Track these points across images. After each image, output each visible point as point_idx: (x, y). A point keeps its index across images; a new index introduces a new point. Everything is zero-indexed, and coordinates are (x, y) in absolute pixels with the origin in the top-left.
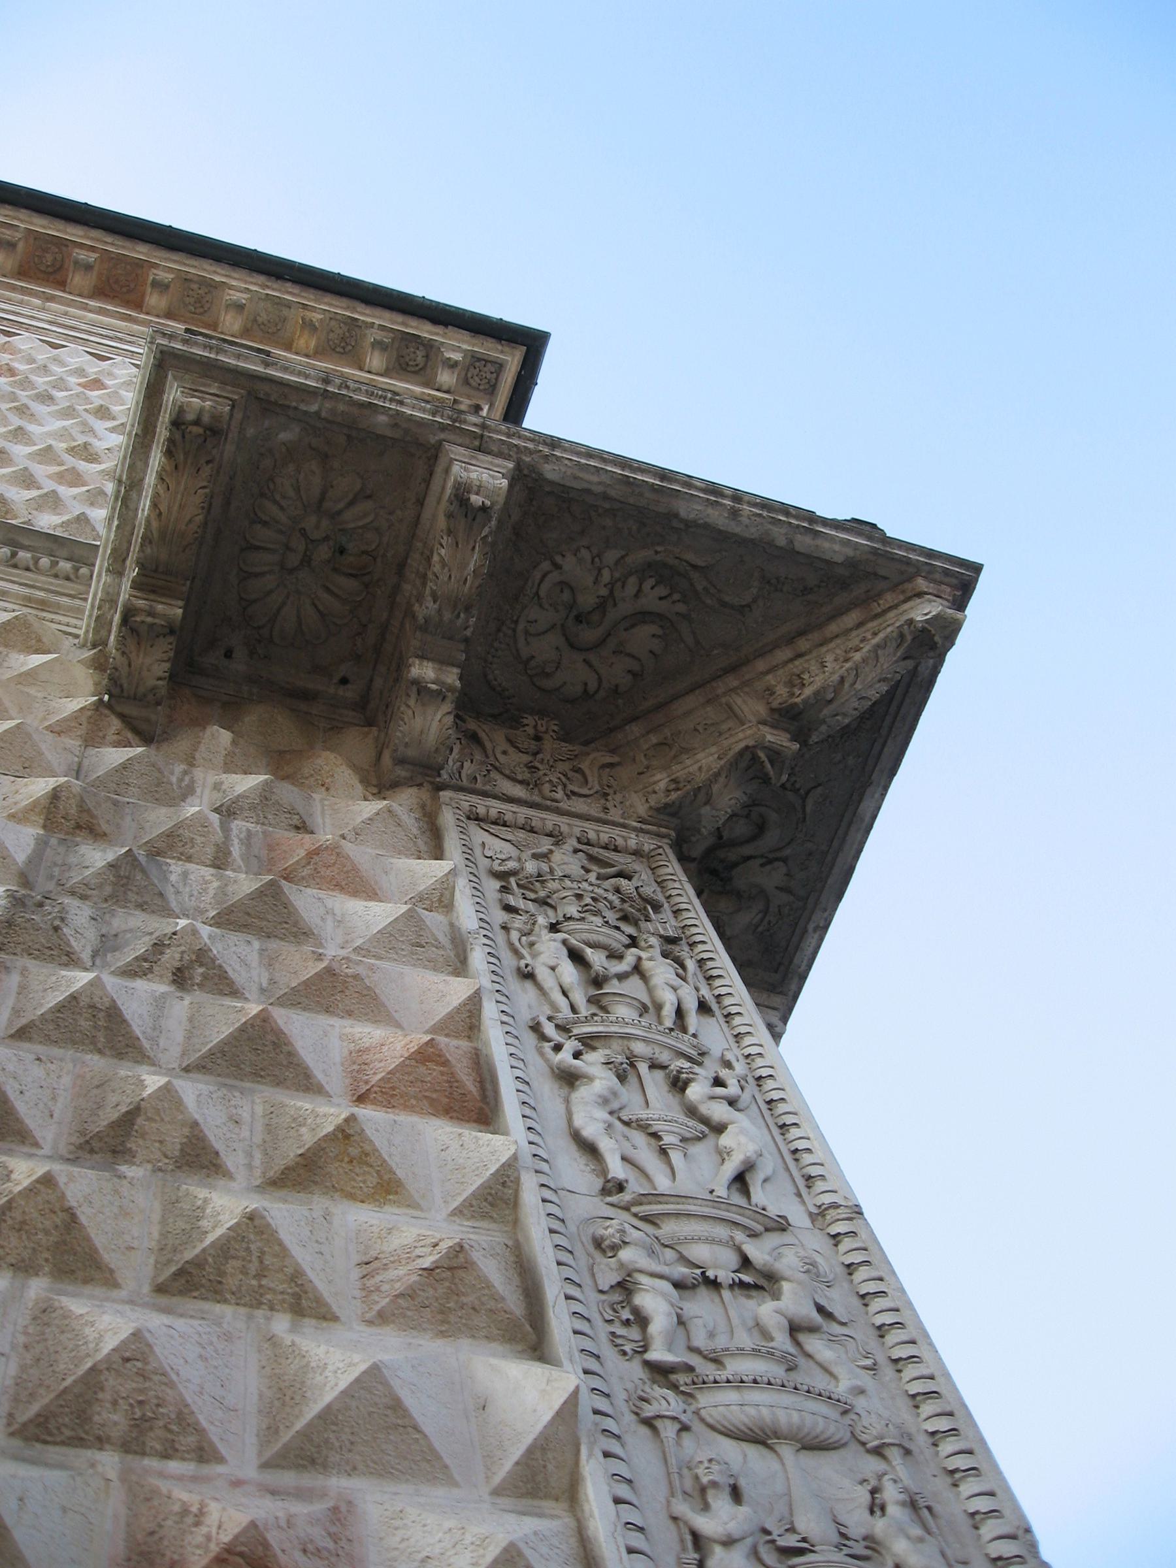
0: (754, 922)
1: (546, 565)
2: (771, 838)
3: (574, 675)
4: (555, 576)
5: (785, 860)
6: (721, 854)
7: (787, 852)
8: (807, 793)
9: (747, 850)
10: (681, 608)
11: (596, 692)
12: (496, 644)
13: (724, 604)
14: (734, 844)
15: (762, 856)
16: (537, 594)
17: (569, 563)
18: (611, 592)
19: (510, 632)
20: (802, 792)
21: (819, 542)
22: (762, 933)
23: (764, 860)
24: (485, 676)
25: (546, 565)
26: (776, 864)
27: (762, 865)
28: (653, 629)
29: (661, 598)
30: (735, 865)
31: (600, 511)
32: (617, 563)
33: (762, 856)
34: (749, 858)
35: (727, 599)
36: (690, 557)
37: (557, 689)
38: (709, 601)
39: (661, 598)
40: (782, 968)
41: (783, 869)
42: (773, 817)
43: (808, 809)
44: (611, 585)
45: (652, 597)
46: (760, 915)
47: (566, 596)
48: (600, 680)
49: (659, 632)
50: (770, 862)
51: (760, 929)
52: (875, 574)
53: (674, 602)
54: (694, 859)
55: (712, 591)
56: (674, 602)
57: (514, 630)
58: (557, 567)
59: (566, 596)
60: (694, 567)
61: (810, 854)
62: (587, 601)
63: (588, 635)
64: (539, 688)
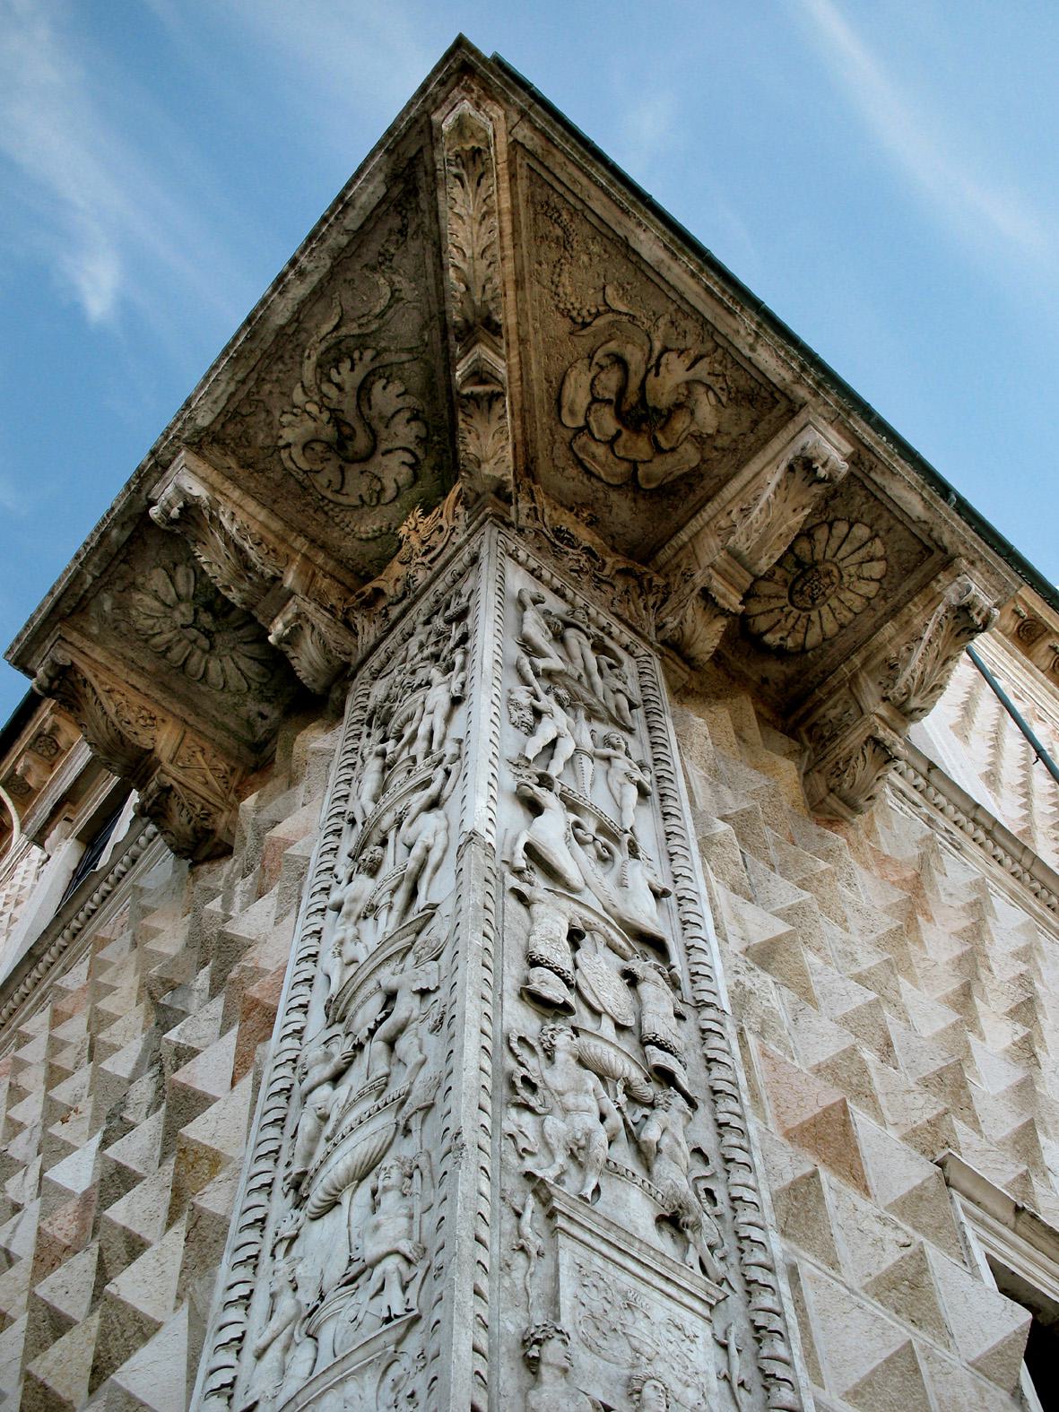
0: (713, 401)
1: (284, 454)
2: (635, 356)
4: (296, 452)
5: (665, 350)
6: (626, 407)
7: (658, 346)
8: (606, 304)
9: (634, 383)
10: (369, 354)
12: (337, 520)
13: (382, 315)
14: (622, 391)
15: (648, 371)
16: (305, 472)
17: (288, 435)
18: (328, 409)
19: (331, 506)
20: (601, 309)
21: (358, 204)
22: (729, 399)
23: (653, 371)
24: (361, 539)
25: (284, 454)
26: (663, 361)
29: (352, 369)
30: (642, 399)
31: (254, 390)
32: (305, 393)
33: (648, 371)
35: (377, 310)
36: (327, 328)
37: (398, 488)
38: (374, 327)
39: (352, 369)
40: (777, 395)
41: (671, 357)
42: (612, 346)
43: (623, 309)
44: (321, 407)
45: (348, 376)
46: (711, 394)
48: (405, 449)
49: (383, 382)
50: (658, 365)
51: (724, 399)
52: (411, 159)
53: (361, 359)
54: (619, 433)
55: (364, 320)
56: (361, 359)
57: (330, 501)
58: (288, 446)
59: (318, 447)
60: (337, 328)
61: (672, 323)
62: (329, 432)
63: (361, 442)
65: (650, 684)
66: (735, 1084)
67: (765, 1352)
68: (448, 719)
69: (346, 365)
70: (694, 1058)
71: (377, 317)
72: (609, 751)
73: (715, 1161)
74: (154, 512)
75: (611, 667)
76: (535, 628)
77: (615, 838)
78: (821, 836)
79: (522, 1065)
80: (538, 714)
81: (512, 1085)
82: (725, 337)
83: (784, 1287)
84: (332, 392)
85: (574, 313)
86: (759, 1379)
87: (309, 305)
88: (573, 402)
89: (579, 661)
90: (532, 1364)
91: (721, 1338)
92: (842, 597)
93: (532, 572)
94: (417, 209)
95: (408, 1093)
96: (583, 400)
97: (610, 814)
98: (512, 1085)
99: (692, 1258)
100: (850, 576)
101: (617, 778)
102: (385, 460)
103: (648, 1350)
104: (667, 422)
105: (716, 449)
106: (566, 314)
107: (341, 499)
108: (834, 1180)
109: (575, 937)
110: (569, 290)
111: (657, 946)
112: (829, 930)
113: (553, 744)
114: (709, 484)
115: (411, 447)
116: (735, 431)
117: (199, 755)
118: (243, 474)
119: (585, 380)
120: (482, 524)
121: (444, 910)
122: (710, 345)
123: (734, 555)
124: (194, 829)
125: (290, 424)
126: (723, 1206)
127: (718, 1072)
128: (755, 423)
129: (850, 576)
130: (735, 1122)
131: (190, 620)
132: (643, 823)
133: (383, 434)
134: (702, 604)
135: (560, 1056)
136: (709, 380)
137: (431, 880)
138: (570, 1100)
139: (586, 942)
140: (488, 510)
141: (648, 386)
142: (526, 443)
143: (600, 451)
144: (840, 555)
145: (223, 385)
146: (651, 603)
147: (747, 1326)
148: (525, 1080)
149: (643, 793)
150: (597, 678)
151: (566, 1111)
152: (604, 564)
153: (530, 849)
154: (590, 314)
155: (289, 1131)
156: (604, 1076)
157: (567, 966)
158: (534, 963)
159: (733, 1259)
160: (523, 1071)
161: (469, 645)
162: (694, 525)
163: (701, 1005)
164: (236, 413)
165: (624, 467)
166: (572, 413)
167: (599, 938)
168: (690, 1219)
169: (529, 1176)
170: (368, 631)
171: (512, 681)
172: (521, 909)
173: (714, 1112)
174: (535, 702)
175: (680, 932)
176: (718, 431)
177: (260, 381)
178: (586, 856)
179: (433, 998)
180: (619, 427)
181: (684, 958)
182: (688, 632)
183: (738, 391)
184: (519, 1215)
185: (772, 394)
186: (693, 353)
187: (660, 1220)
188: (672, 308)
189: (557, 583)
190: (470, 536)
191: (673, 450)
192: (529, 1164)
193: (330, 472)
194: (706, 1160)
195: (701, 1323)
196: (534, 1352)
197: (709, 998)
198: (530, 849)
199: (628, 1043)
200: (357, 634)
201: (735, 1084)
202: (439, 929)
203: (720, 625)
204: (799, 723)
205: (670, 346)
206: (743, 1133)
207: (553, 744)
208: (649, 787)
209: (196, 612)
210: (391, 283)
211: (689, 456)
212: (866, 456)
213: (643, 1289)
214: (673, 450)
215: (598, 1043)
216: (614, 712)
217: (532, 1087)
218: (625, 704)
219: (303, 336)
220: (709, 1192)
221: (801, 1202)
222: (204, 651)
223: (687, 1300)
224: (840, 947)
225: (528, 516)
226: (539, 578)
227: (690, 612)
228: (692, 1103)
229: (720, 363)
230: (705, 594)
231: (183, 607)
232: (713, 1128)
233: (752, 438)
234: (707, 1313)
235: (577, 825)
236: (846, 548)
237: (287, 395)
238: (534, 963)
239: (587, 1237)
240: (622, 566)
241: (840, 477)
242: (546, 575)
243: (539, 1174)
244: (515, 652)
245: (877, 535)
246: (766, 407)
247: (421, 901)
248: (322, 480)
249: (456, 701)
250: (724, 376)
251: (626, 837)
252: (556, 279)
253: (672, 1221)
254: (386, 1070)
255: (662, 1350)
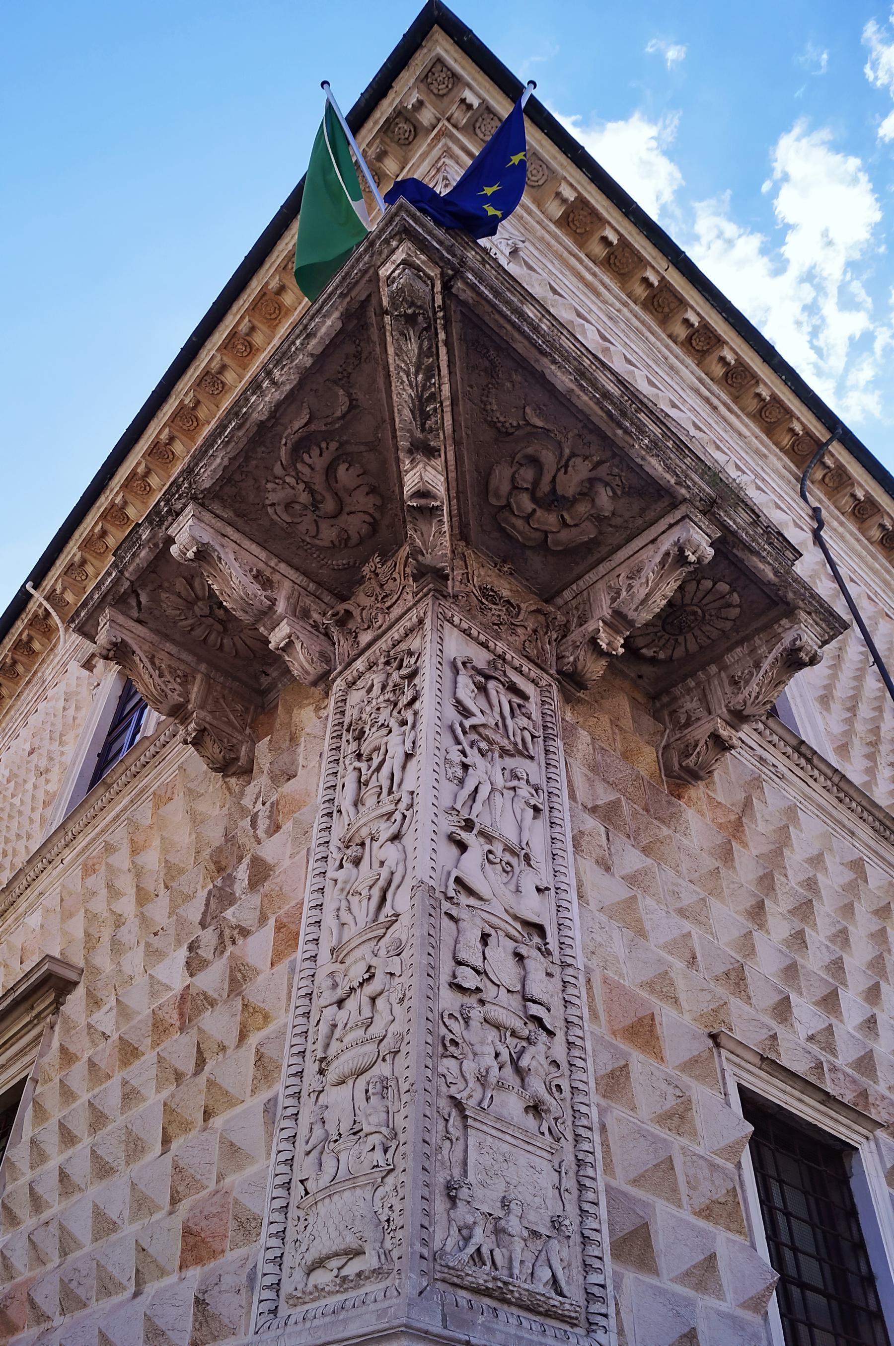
1: (270, 510)
2: (548, 457)
3: (355, 524)
4: (279, 509)
5: (573, 455)
6: (539, 494)
7: (567, 451)
8: (526, 420)
9: (547, 478)
10: (333, 446)
11: (374, 518)
13: (343, 416)
14: (536, 483)
15: (558, 470)
17: (272, 498)
21: (319, 335)
22: (623, 493)
23: (563, 470)
26: (571, 463)
27: (566, 473)
28: (342, 469)
29: (321, 455)
30: (554, 490)
33: (558, 470)
34: (554, 477)
35: (338, 414)
36: (297, 425)
38: (337, 426)
39: (321, 455)
40: (662, 493)
41: (579, 460)
42: (530, 450)
43: (540, 423)
44: (298, 479)
45: (316, 460)
46: (608, 489)
47: (297, 507)
49: (346, 465)
50: (566, 466)
51: (619, 492)
52: (363, 302)
54: (534, 511)
55: (330, 420)
58: (273, 505)
60: (306, 425)
62: (304, 498)
64: (358, 545)
65: (549, 712)
66: (581, 1018)
67: (581, 1173)
68: (404, 768)
69: (315, 452)
70: (556, 1003)
71: (339, 419)
72: (515, 783)
73: (564, 1065)
74: (174, 550)
75: (519, 706)
76: (466, 690)
77: (513, 853)
78: (669, 802)
79: (451, 1031)
80: (465, 767)
81: (444, 1045)
82: (622, 449)
83: (597, 1138)
84: (306, 470)
85: (499, 425)
86: (576, 1186)
87: (284, 406)
88: (498, 488)
89: (497, 709)
90: (453, 1200)
91: (557, 1167)
92: (704, 629)
93: (464, 631)
94: (369, 339)
95: (385, 1037)
96: (505, 487)
97: (512, 837)
98: (444, 1045)
99: (544, 1129)
100: (711, 616)
101: (520, 805)
102: (350, 518)
103: (514, 1182)
104: (572, 506)
105: (611, 526)
106: (492, 424)
107: (317, 542)
108: (642, 1057)
109: (485, 938)
110: (495, 407)
111: (540, 930)
112: (664, 877)
113: (476, 790)
114: (604, 550)
115: (371, 511)
116: (627, 515)
117: (221, 701)
118: (240, 522)
119: (508, 472)
120: (426, 595)
121: (404, 920)
122: (609, 454)
123: (618, 614)
124: (224, 757)
125: (274, 490)
126: (567, 1093)
127: (572, 1010)
128: (643, 510)
129: (711, 616)
130: (579, 1042)
131: (207, 611)
132: (537, 837)
133: (347, 500)
134: (592, 648)
135: (472, 1023)
136: (608, 479)
137: (395, 894)
138: (478, 1048)
139: (492, 941)
140: (431, 585)
141: (558, 480)
142: (460, 514)
143: (519, 523)
144: (704, 602)
145: (218, 460)
146: (555, 637)
147: (573, 1158)
148: (452, 1041)
149: (536, 809)
150: (509, 721)
151: (475, 1054)
152: (520, 609)
153: (458, 880)
154: (512, 426)
155: (313, 1021)
156: (497, 1026)
157: (479, 963)
158: (460, 963)
159: (569, 1123)
160: (452, 1036)
161: (417, 705)
162: (591, 577)
163: (564, 965)
164: (229, 480)
165: (537, 535)
166: (497, 496)
167: (499, 932)
168: (545, 1108)
169: (452, 1097)
170: (344, 646)
171: (447, 740)
172: (452, 925)
173: (566, 1034)
174: (464, 759)
175: (554, 912)
176: (613, 514)
177: (247, 458)
178: (495, 874)
179: (397, 980)
180: (534, 506)
181: (556, 931)
182: (580, 667)
183: (630, 488)
184: (447, 1121)
185: (658, 491)
186: (596, 459)
187: (527, 1109)
188: (580, 425)
189: (482, 638)
190: (418, 601)
191: (576, 525)
192: (453, 1091)
193: (306, 524)
194: (558, 1066)
195: (546, 1162)
196: (453, 1193)
197: (570, 960)
198: (458, 880)
199: (515, 1002)
200: (334, 644)
201: (581, 1018)
202: (399, 931)
203: (604, 662)
204: (664, 706)
205: (577, 452)
206: (583, 1049)
207: (476, 790)
208: (541, 806)
209: (211, 608)
210: (349, 395)
211: (589, 532)
212: (730, 538)
213: (514, 1150)
214: (576, 525)
215: (497, 1008)
216: (520, 747)
217: (454, 1042)
218: (528, 738)
219: (279, 428)
220: (558, 1087)
221: (616, 1082)
222: (219, 633)
223: (539, 1152)
224: (671, 888)
225: (461, 582)
226: (469, 635)
227: (583, 653)
228: (551, 1033)
229: (617, 467)
230: (593, 641)
231: (200, 604)
232: (565, 1045)
233: (640, 521)
234: (549, 1157)
235: (490, 852)
236: (709, 598)
237: (269, 469)
238: (460, 963)
239: (484, 1128)
240: (533, 608)
241: (706, 561)
242: (474, 632)
243: (458, 1096)
244: (451, 714)
245: (735, 591)
246: (654, 499)
247: (387, 910)
248: (302, 528)
249: (408, 756)
250: (620, 477)
251: (523, 852)
252: (484, 399)
253: (536, 1109)
254: (370, 1015)
255: (522, 1180)
